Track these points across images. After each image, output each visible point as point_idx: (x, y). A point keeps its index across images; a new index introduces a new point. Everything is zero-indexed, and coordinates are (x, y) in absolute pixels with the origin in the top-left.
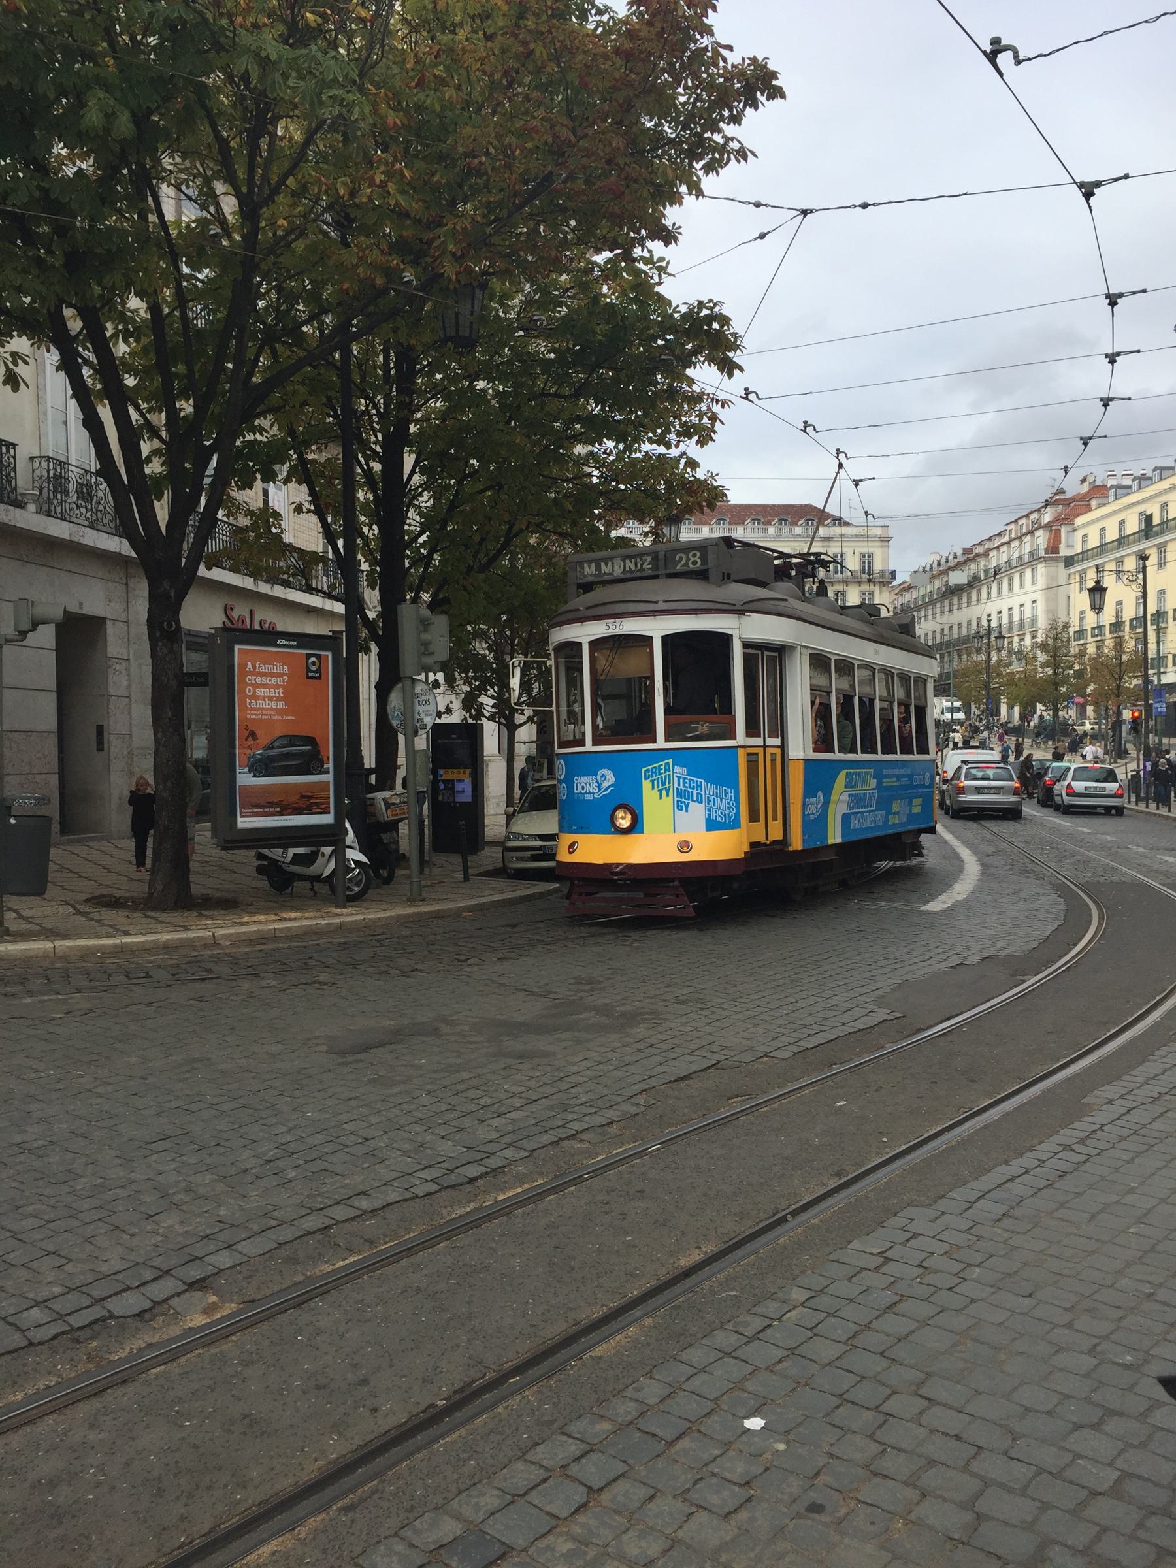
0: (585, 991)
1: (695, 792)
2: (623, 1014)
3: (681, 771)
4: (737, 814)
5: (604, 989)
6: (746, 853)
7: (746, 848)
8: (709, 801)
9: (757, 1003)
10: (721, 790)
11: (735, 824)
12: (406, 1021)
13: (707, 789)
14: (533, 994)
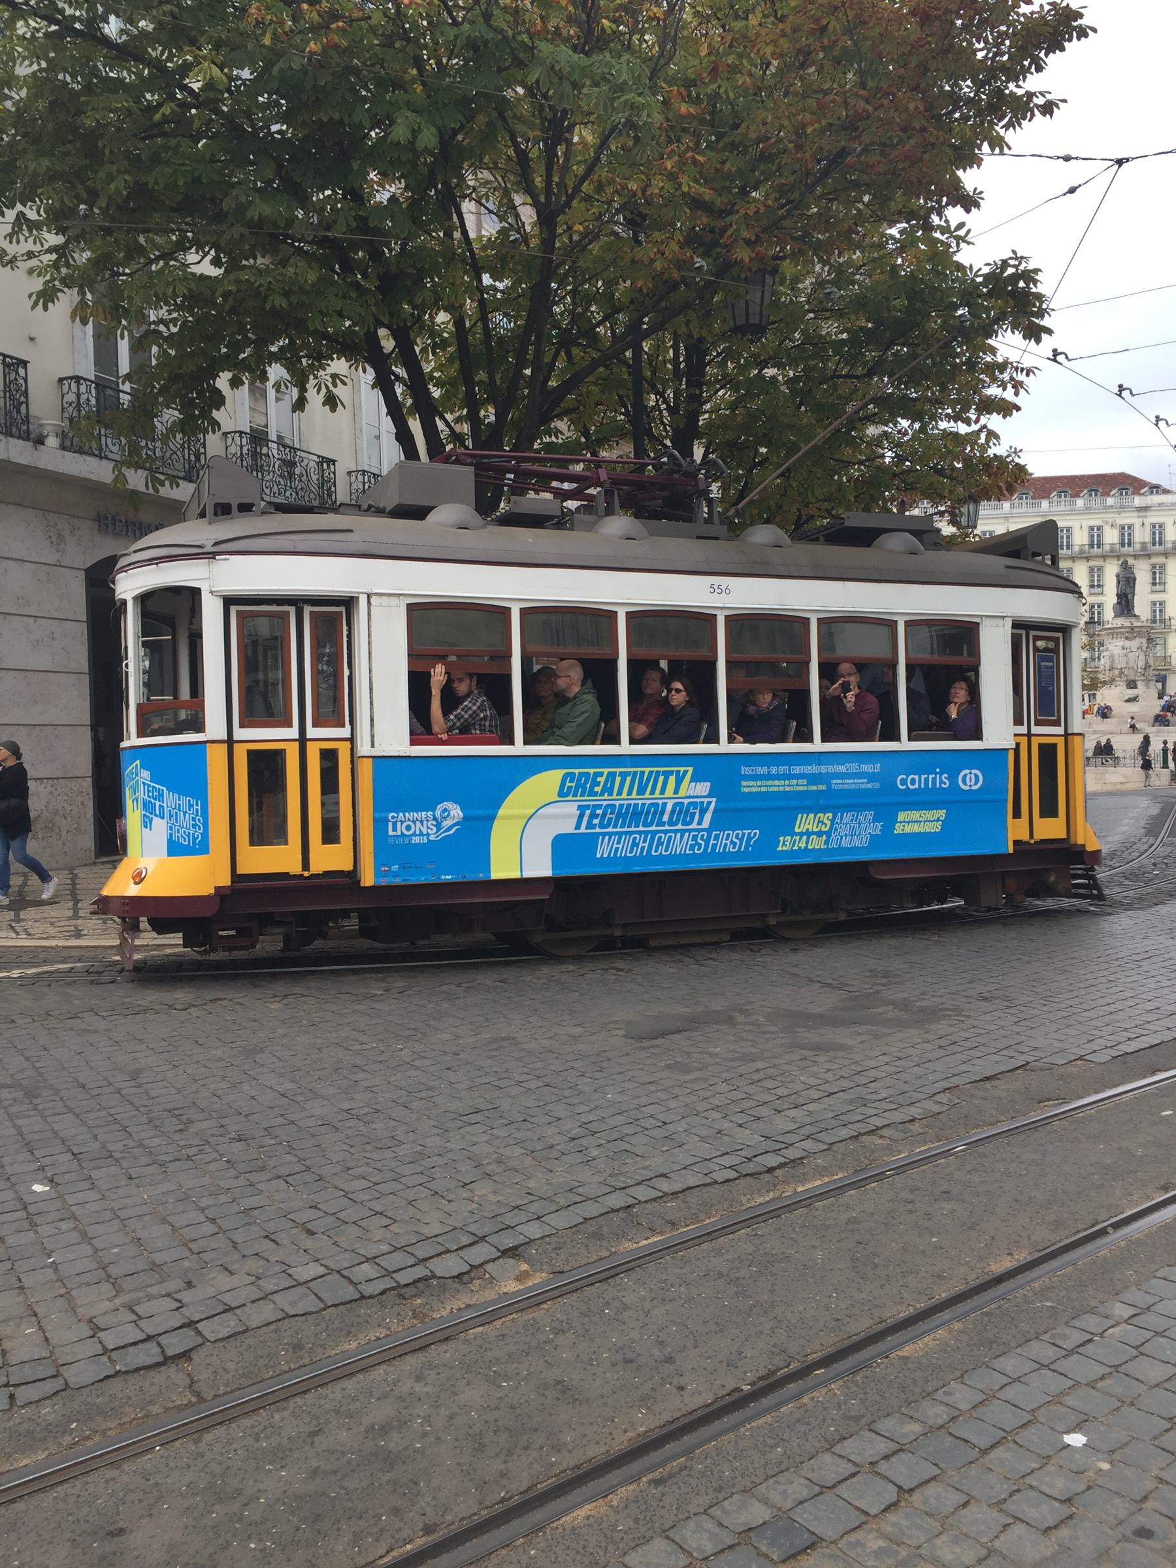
0: (882, 985)
1: (158, 803)
2: (922, 1010)
3: (146, 774)
4: (205, 834)
5: (902, 983)
6: (217, 888)
7: (225, 880)
8: (171, 816)
9: (1069, 1003)
10: (185, 801)
11: (201, 847)
12: (700, 1009)
13: (170, 800)
14: (828, 985)
